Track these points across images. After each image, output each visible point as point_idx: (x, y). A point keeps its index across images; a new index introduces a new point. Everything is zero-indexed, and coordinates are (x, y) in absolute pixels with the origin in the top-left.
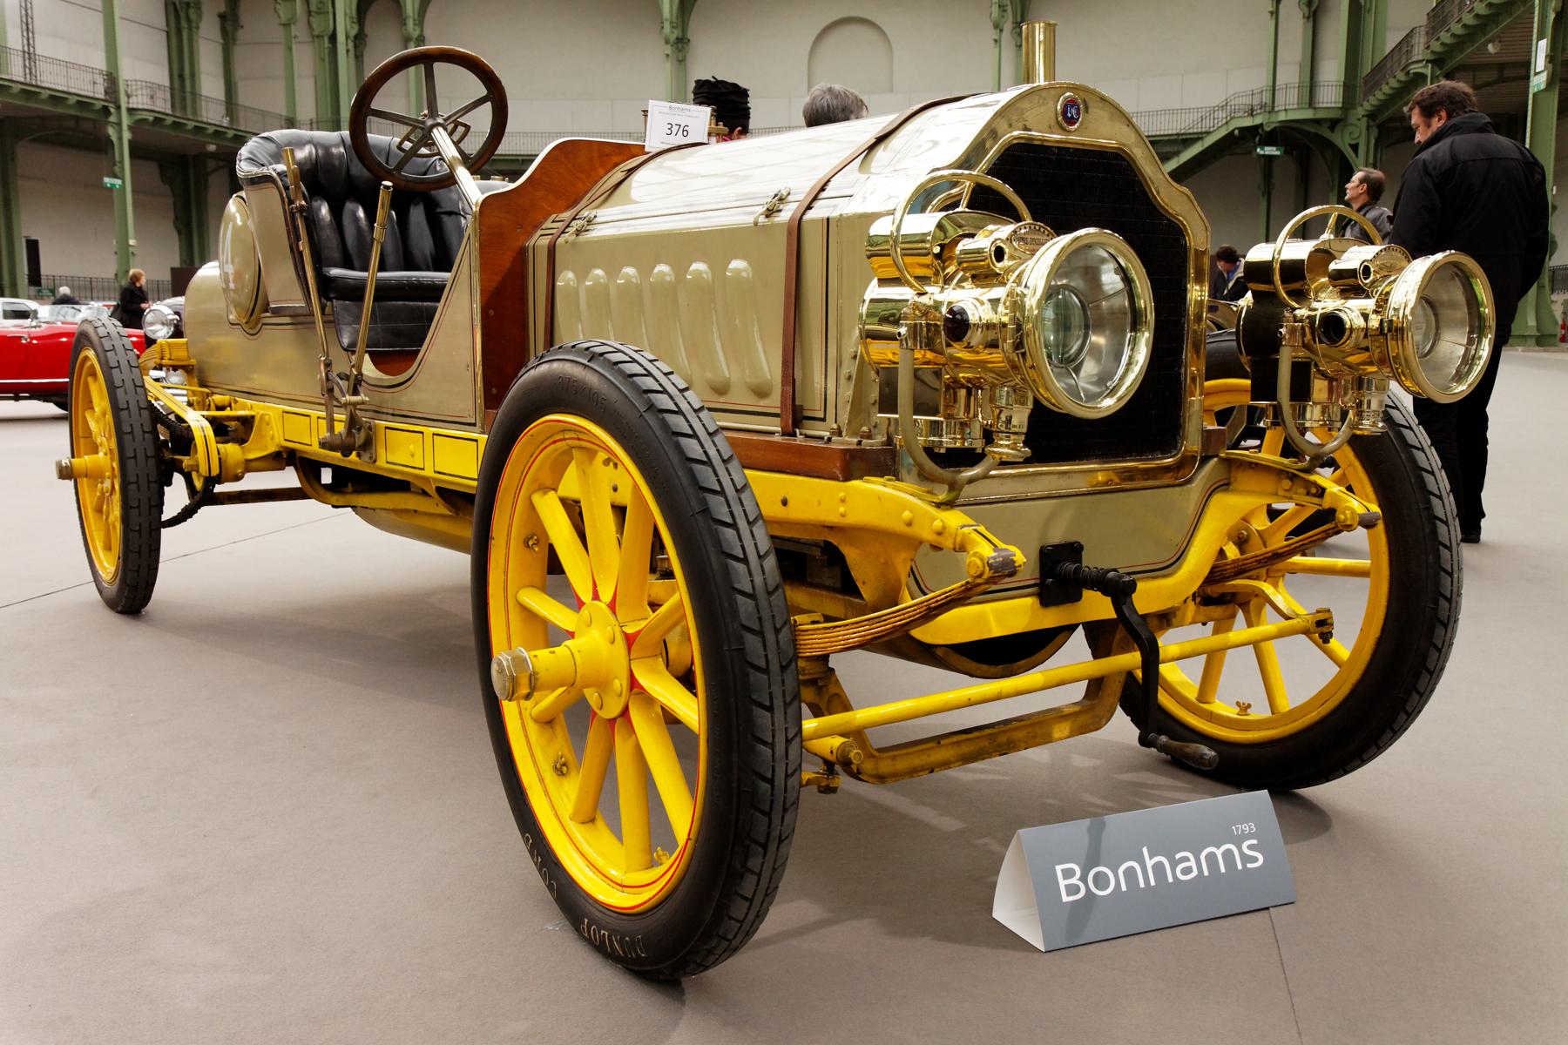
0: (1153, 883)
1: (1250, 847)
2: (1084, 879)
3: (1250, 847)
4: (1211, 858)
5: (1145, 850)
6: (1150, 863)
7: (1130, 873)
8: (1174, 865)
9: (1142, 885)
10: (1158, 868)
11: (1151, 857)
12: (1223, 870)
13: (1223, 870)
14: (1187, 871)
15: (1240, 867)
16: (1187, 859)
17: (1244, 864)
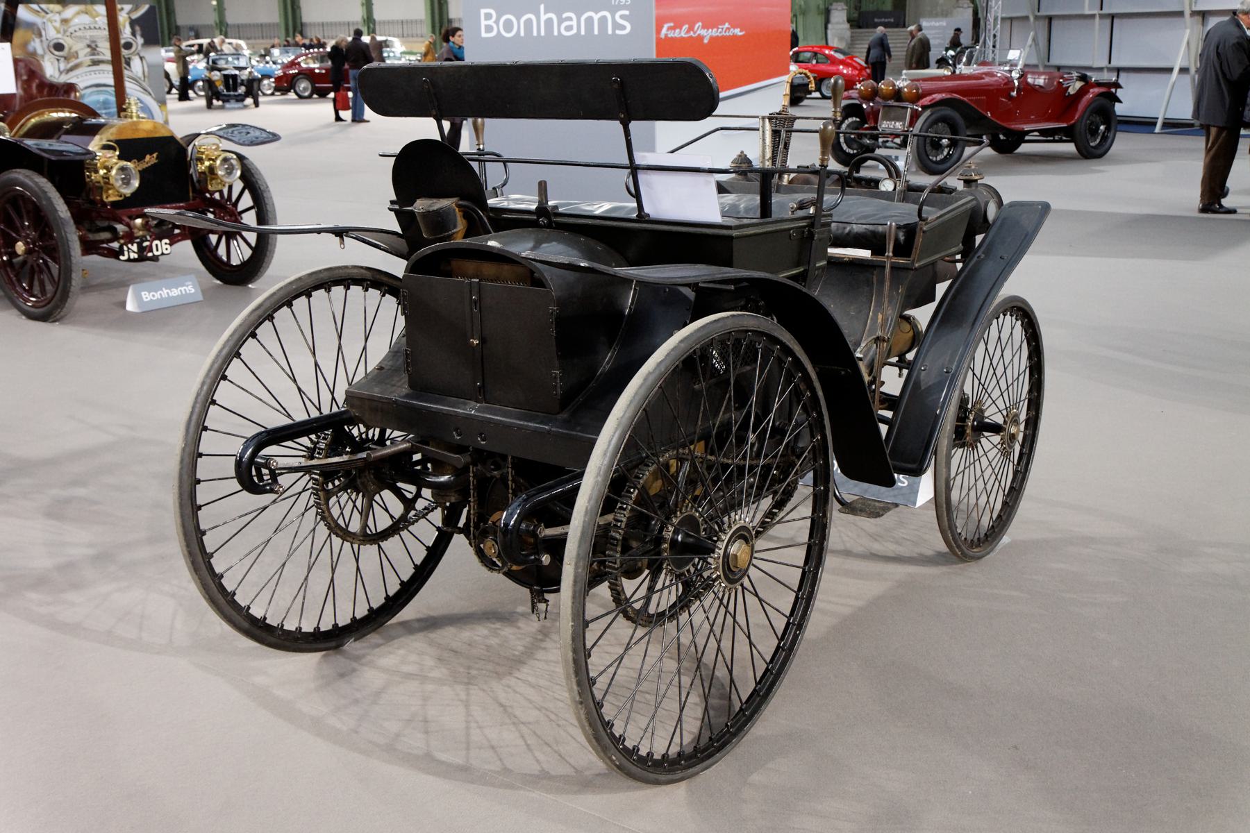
0: (543, 33)
1: (622, 17)
2: (497, 22)
3: (622, 17)
4: (590, 20)
6: (543, 18)
7: (529, 22)
8: (561, 21)
9: (535, 34)
10: (549, 22)
11: (546, 13)
12: (596, 32)
13: (596, 32)
14: (569, 28)
15: (610, 32)
17: (614, 30)
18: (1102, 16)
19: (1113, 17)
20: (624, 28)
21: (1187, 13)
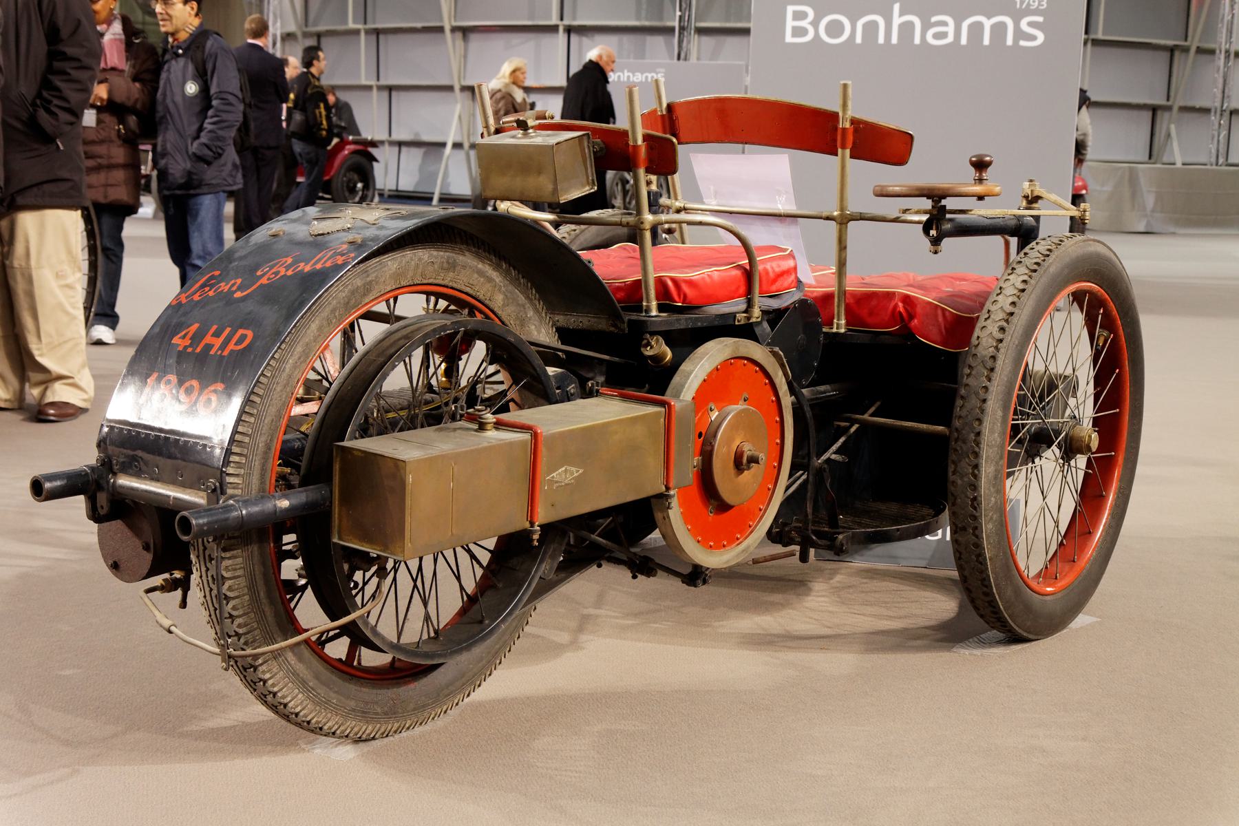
0: (894, 40)
1: (1030, 24)
3: (1030, 24)
4: (976, 29)
5: (897, 7)
6: (897, 20)
8: (926, 26)
9: (881, 40)
10: (907, 28)
11: (901, 15)
12: (986, 41)
13: (986, 41)
14: (938, 36)
15: (1010, 42)
16: (945, 24)
17: (1016, 40)
18: (380, 88)
19: (390, 89)
20: (1034, 38)
21: (457, 88)
